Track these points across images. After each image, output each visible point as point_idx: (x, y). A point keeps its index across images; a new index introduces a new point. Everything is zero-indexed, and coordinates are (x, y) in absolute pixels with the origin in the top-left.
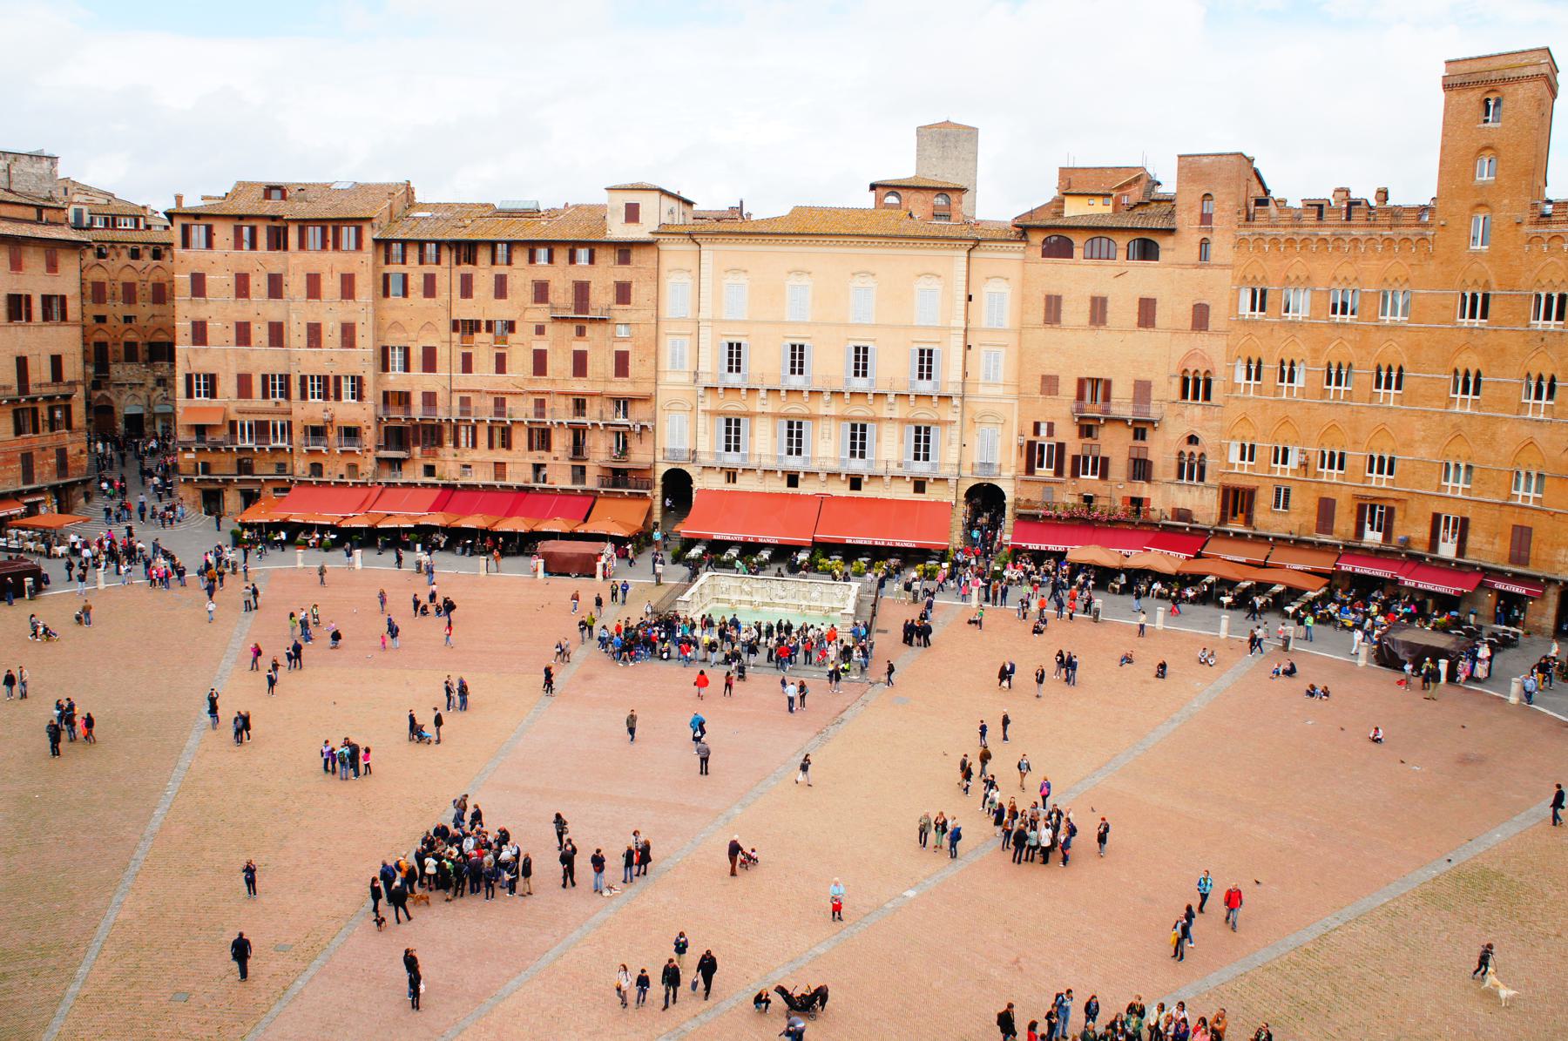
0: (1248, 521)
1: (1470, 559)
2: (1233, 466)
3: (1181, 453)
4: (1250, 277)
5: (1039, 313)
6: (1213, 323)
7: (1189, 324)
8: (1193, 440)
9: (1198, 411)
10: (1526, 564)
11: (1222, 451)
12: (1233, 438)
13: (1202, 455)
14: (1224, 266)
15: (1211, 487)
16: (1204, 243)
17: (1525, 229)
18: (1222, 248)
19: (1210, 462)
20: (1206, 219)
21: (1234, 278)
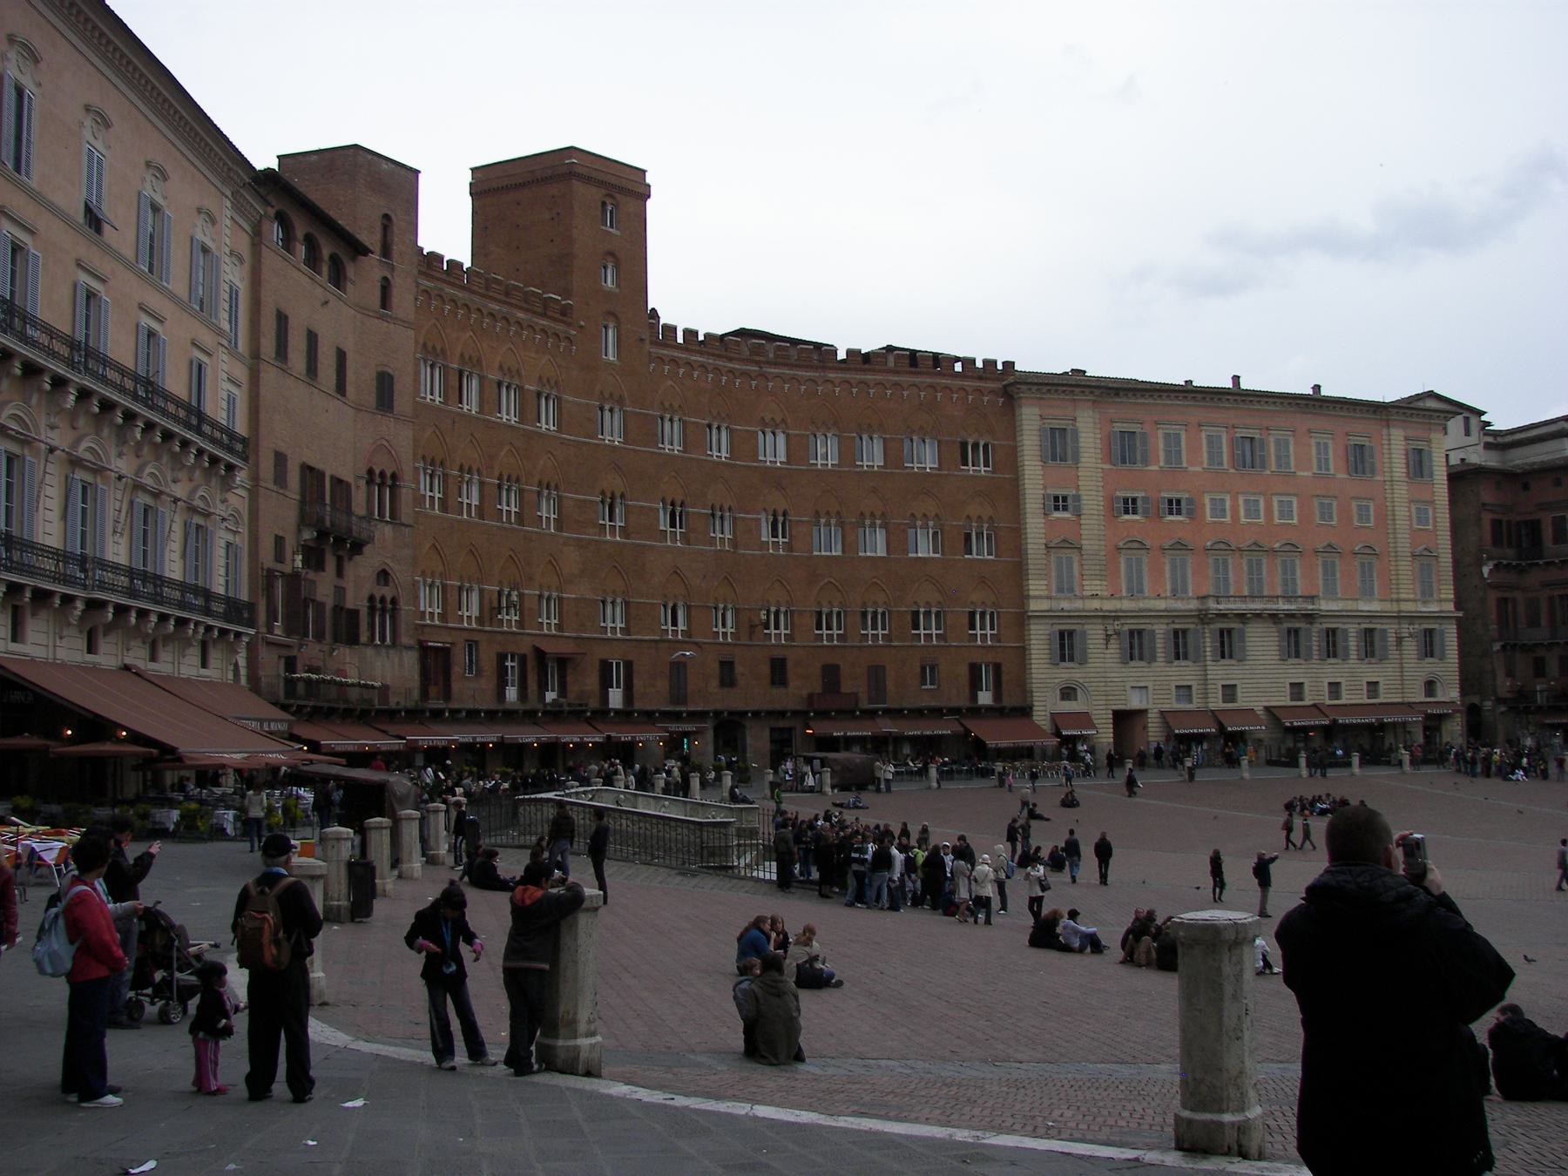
0: (447, 694)
1: (638, 706)
2: (424, 613)
3: (371, 598)
4: (430, 345)
5: (268, 345)
6: (402, 402)
7: (371, 399)
8: (384, 576)
9: (388, 530)
10: (685, 703)
11: (417, 598)
12: (423, 574)
13: (394, 601)
14: (406, 324)
15: (410, 648)
16: (386, 287)
17: (647, 346)
18: (404, 299)
19: (405, 607)
20: (386, 251)
21: (416, 342)
